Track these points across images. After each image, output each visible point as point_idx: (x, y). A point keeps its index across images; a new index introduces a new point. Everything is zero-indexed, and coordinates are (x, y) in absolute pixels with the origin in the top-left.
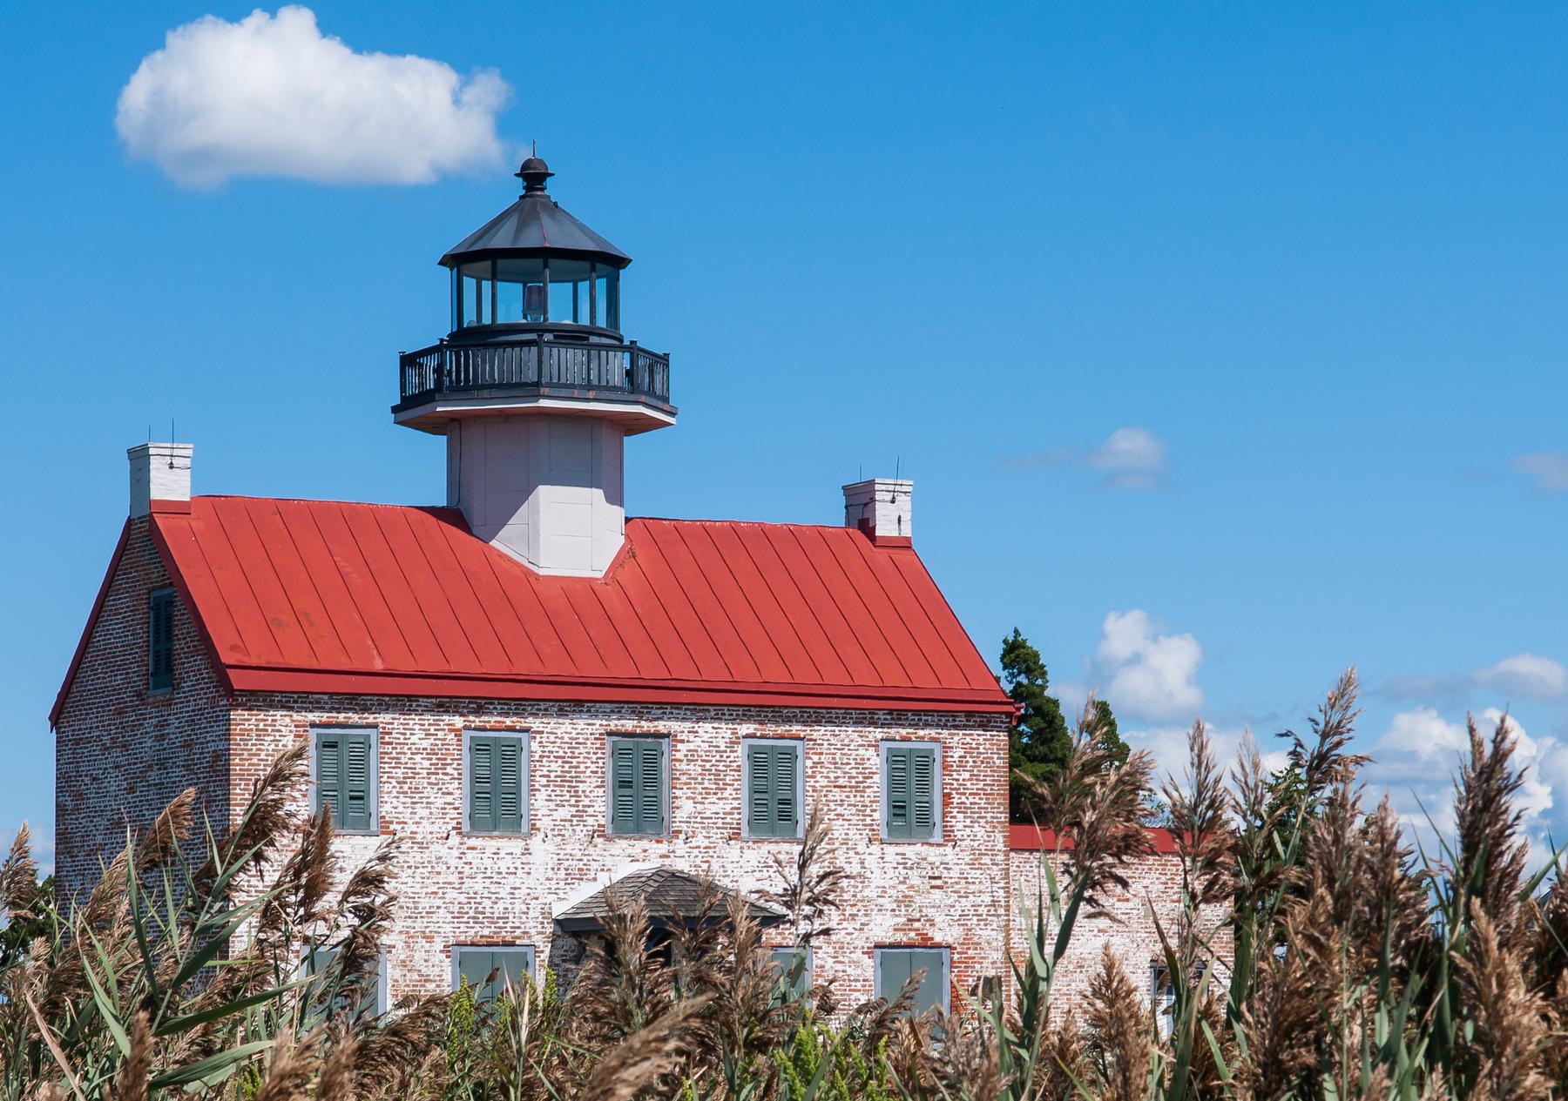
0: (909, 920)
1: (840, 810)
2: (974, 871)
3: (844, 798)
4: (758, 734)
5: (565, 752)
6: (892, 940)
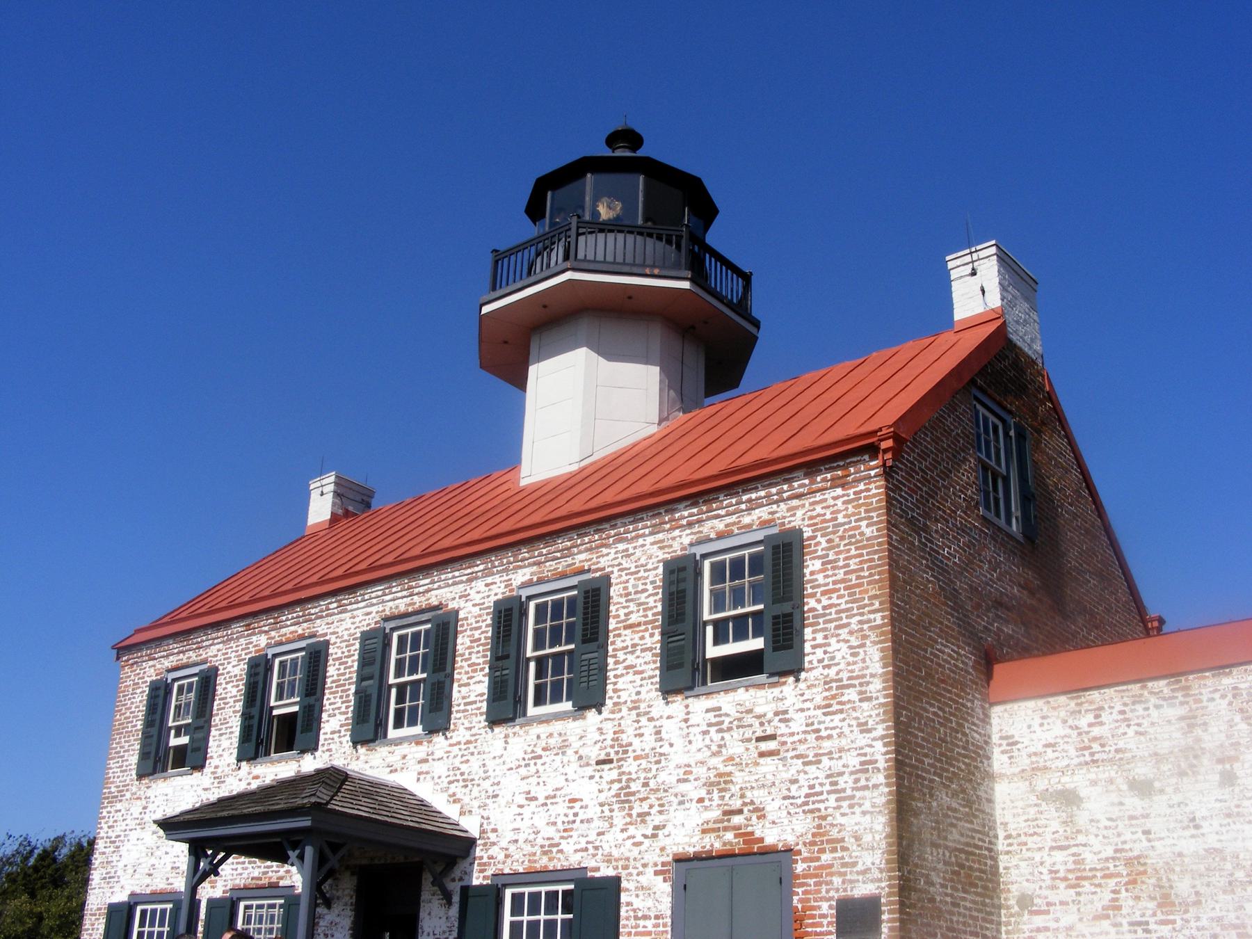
0: (726, 813)
1: (631, 659)
2: (829, 718)
3: (637, 641)
4: (535, 579)
5: (343, 653)
6: (698, 849)
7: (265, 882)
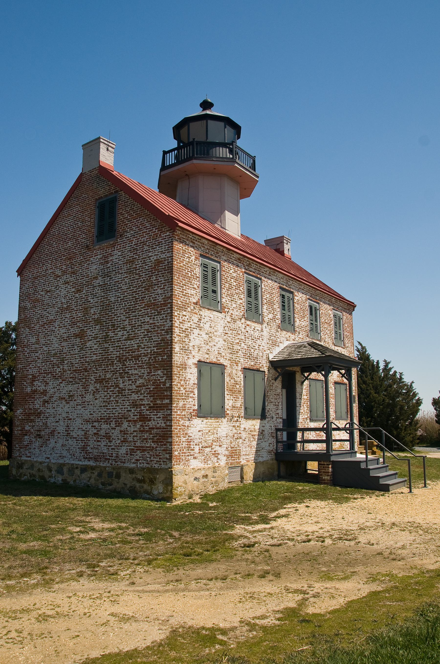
7: (255, 368)
